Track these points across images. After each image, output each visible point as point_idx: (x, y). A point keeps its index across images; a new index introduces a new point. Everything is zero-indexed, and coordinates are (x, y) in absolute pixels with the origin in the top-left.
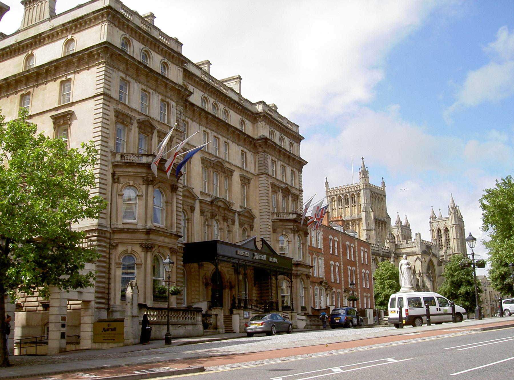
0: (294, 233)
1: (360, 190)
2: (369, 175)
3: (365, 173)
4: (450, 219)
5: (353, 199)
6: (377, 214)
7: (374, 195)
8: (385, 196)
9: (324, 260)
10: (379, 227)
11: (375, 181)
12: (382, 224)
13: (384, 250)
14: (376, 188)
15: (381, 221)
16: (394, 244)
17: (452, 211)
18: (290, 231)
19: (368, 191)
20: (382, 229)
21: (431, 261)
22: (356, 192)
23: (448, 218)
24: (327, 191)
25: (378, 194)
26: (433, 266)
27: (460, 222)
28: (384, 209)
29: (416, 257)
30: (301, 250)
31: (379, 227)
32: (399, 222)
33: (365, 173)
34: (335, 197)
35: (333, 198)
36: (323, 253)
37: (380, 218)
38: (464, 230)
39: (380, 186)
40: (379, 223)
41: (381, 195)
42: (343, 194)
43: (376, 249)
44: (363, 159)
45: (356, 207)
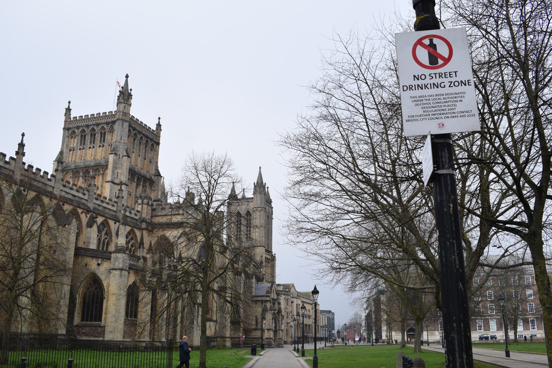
1: (114, 122)
2: (134, 101)
3: (125, 96)
4: (255, 200)
5: (103, 135)
8: (158, 144)
11: (142, 112)
12: (144, 182)
17: (258, 189)
19: (126, 125)
22: (107, 123)
23: (252, 198)
24: (65, 121)
27: (267, 208)
28: (154, 161)
29: (181, 231)
33: (125, 96)
34: (76, 131)
37: (144, 172)
38: (272, 219)
39: (154, 127)
40: (139, 180)
41: (151, 140)
42: (88, 126)
43: (110, 207)
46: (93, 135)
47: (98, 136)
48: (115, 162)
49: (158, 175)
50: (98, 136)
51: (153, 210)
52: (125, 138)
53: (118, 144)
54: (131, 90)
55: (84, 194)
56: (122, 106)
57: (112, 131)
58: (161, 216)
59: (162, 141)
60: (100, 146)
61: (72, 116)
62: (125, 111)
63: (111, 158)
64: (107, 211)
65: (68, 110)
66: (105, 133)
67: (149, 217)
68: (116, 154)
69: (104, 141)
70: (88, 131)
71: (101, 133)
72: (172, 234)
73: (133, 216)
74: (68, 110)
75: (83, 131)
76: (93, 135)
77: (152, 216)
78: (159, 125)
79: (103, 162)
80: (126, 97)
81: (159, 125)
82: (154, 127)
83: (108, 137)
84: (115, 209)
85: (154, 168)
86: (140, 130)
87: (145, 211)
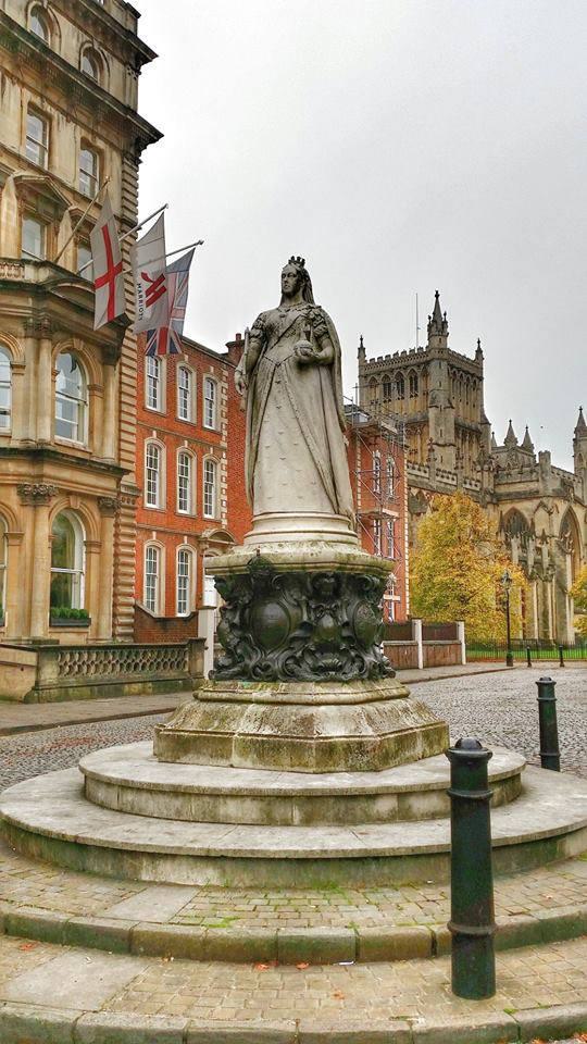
0: (39, 340)
1: (428, 363)
3: (438, 326)
5: (414, 380)
6: (461, 413)
7: (458, 375)
8: (481, 379)
9: (229, 468)
10: (463, 440)
11: (460, 343)
13: (468, 486)
14: (463, 359)
15: (470, 428)
16: (491, 475)
18: (21, 330)
19: (444, 364)
20: (470, 446)
21: (570, 513)
25: (467, 373)
26: (576, 524)
28: (477, 405)
29: (537, 502)
30: (87, 410)
31: (463, 440)
32: (510, 438)
33: (438, 326)
35: (374, 379)
36: (224, 445)
39: (472, 357)
40: (464, 435)
41: (473, 375)
42: (392, 371)
44: (437, 296)
45: (418, 399)
46: (400, 383)
47: (407, 383)
48: (437, 418)
49: (486, 423)
50: (407, 383)
51: (496, 477)
52: (445, 384)
53: (437, 392)
54: (445, 314)
55: (425, 472)
56: (436, 341)
57: (426, 374)
58: (507, 483)
59: (485, 375)
60: (411, 396)
61: (368, 358)
62: (442, 346)
63: (432, 413)
64: (448, 487)
65: (362, 349)
66: (416, 378)
67: (491, 487)
68: (437, 407)
69: (416, 389)
70: (392, 377)
71: (411, 378)
72: (525, 507)
73: (474, 488)
74: (362, 349)
75: (386, 377)
76: (400, 383)
77: (495, 485)
78: (479, 352)
79: (419, 417)
80: (440, 327)
81: (479, 352)
82: (472, 357)
83: (421, 383)
84: (454, 483)
85: (479, 414)
86: (465, 369)
87: (486, 480)
